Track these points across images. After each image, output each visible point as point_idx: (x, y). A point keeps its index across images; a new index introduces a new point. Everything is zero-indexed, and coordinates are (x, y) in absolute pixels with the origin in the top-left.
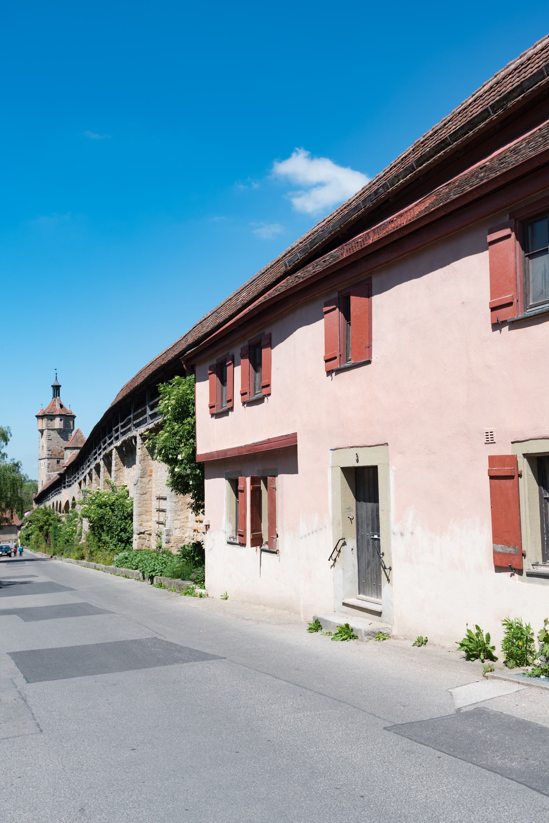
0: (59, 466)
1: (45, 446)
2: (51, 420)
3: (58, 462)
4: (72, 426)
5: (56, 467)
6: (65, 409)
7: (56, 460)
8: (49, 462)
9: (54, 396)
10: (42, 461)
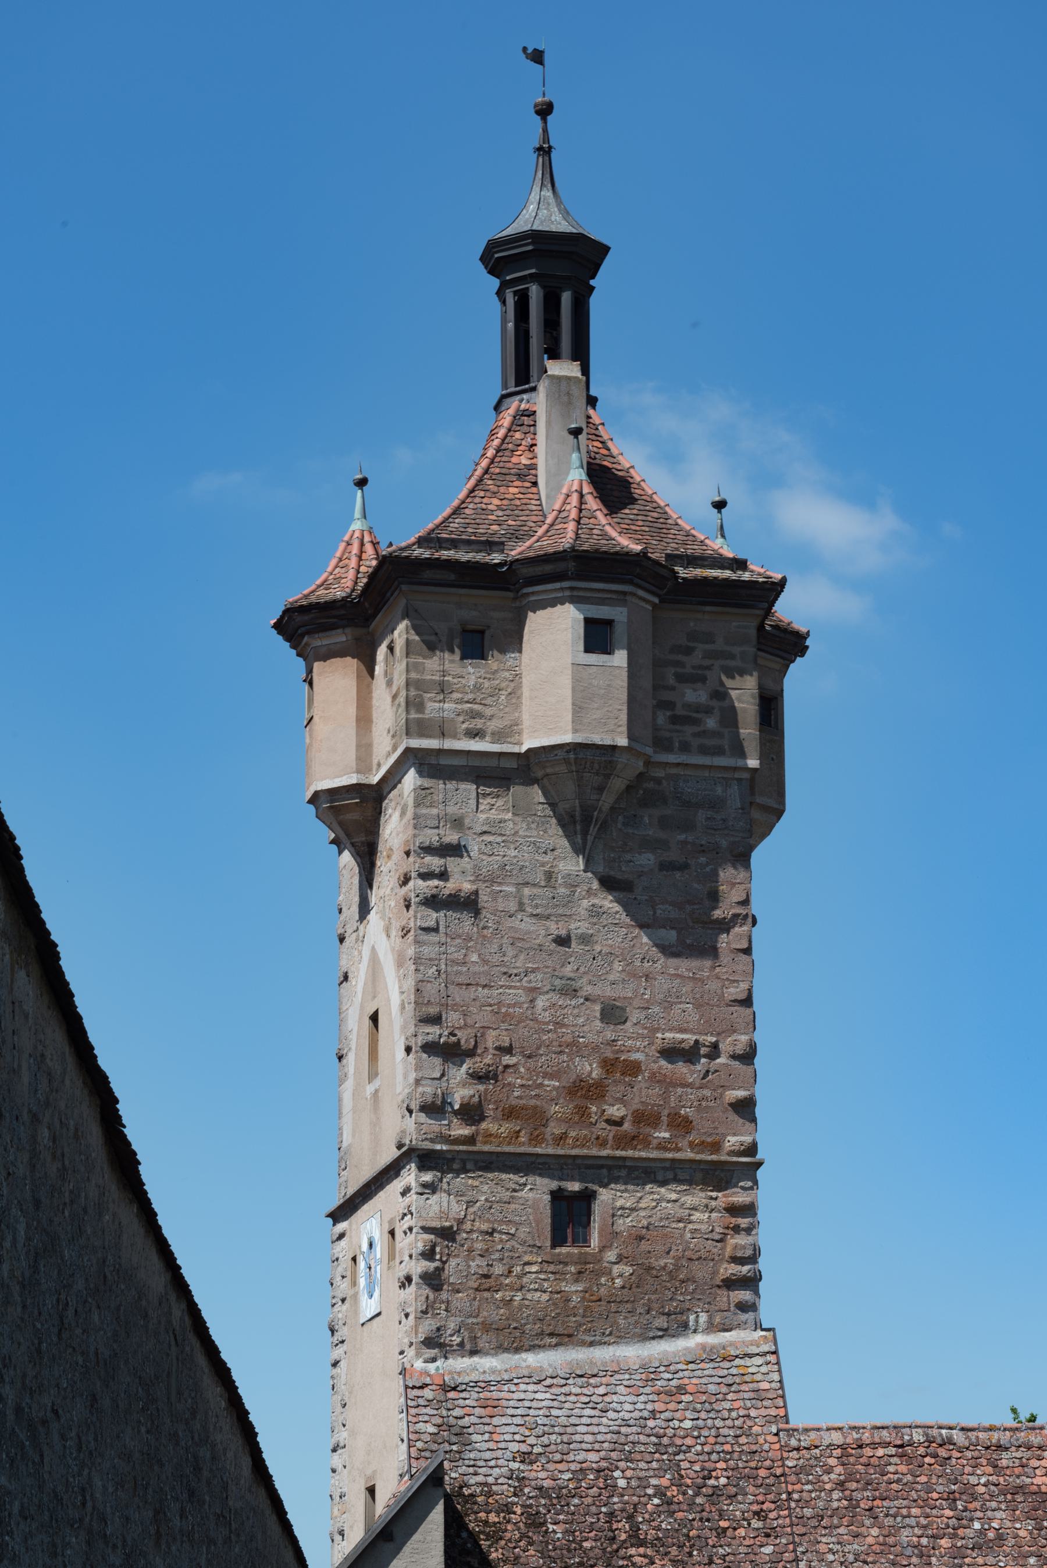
0: (588, 1269)
1: (395, 997)
2: (475, 644)
3: (570, 1215)
4: (749, 731)
5: (535, 1290)
6: (660, 521)
7: (536, 1193)
8: (441, 1207)
9: (522, 374)
10: (369, 1225)
